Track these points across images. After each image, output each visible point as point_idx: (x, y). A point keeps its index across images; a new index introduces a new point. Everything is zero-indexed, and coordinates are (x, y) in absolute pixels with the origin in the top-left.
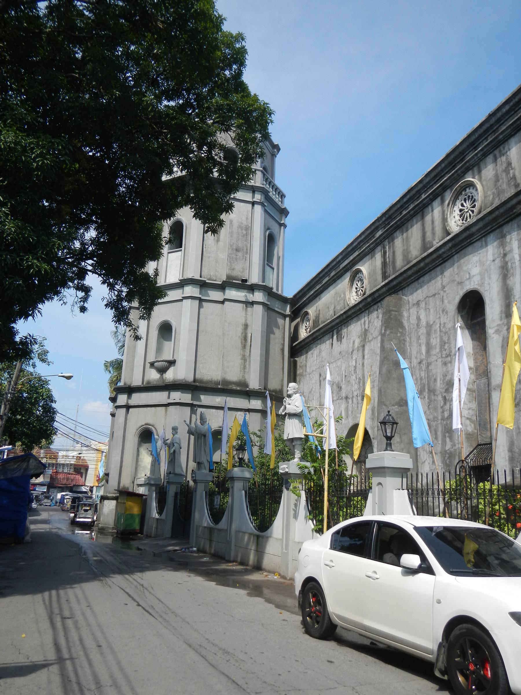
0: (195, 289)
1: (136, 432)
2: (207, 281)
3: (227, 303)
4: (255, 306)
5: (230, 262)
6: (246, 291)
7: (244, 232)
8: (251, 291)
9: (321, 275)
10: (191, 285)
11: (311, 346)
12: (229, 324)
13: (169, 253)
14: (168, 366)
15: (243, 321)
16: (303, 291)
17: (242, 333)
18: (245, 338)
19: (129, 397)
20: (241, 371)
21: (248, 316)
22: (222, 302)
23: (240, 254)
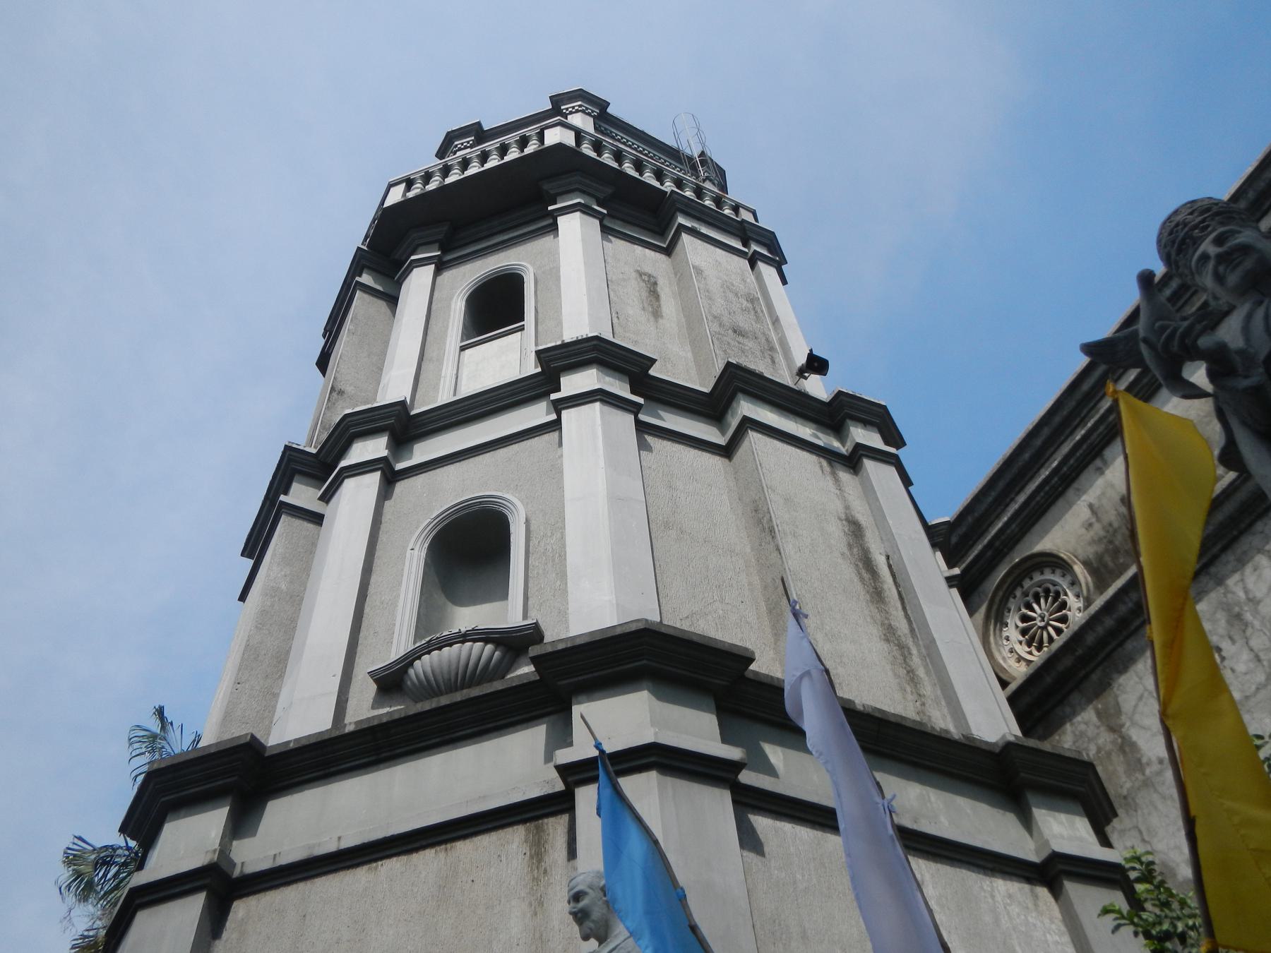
0: (611, 379)
2: (653, 372)
3: (753, 437)
4: (869, 465)
5: (725, 351)
6: (814, 426)
8: (829, 431)
9: (1086, 387)
10: (595, 366)
11: (1129, 645)
13: (463, 349)
14: (500, 661)
15: (838, 506)
16: (970, 519)
17: (850, 546)
19: (241, 823)
21: (851, 498)
22: (727, 451)
23: (749, 344)
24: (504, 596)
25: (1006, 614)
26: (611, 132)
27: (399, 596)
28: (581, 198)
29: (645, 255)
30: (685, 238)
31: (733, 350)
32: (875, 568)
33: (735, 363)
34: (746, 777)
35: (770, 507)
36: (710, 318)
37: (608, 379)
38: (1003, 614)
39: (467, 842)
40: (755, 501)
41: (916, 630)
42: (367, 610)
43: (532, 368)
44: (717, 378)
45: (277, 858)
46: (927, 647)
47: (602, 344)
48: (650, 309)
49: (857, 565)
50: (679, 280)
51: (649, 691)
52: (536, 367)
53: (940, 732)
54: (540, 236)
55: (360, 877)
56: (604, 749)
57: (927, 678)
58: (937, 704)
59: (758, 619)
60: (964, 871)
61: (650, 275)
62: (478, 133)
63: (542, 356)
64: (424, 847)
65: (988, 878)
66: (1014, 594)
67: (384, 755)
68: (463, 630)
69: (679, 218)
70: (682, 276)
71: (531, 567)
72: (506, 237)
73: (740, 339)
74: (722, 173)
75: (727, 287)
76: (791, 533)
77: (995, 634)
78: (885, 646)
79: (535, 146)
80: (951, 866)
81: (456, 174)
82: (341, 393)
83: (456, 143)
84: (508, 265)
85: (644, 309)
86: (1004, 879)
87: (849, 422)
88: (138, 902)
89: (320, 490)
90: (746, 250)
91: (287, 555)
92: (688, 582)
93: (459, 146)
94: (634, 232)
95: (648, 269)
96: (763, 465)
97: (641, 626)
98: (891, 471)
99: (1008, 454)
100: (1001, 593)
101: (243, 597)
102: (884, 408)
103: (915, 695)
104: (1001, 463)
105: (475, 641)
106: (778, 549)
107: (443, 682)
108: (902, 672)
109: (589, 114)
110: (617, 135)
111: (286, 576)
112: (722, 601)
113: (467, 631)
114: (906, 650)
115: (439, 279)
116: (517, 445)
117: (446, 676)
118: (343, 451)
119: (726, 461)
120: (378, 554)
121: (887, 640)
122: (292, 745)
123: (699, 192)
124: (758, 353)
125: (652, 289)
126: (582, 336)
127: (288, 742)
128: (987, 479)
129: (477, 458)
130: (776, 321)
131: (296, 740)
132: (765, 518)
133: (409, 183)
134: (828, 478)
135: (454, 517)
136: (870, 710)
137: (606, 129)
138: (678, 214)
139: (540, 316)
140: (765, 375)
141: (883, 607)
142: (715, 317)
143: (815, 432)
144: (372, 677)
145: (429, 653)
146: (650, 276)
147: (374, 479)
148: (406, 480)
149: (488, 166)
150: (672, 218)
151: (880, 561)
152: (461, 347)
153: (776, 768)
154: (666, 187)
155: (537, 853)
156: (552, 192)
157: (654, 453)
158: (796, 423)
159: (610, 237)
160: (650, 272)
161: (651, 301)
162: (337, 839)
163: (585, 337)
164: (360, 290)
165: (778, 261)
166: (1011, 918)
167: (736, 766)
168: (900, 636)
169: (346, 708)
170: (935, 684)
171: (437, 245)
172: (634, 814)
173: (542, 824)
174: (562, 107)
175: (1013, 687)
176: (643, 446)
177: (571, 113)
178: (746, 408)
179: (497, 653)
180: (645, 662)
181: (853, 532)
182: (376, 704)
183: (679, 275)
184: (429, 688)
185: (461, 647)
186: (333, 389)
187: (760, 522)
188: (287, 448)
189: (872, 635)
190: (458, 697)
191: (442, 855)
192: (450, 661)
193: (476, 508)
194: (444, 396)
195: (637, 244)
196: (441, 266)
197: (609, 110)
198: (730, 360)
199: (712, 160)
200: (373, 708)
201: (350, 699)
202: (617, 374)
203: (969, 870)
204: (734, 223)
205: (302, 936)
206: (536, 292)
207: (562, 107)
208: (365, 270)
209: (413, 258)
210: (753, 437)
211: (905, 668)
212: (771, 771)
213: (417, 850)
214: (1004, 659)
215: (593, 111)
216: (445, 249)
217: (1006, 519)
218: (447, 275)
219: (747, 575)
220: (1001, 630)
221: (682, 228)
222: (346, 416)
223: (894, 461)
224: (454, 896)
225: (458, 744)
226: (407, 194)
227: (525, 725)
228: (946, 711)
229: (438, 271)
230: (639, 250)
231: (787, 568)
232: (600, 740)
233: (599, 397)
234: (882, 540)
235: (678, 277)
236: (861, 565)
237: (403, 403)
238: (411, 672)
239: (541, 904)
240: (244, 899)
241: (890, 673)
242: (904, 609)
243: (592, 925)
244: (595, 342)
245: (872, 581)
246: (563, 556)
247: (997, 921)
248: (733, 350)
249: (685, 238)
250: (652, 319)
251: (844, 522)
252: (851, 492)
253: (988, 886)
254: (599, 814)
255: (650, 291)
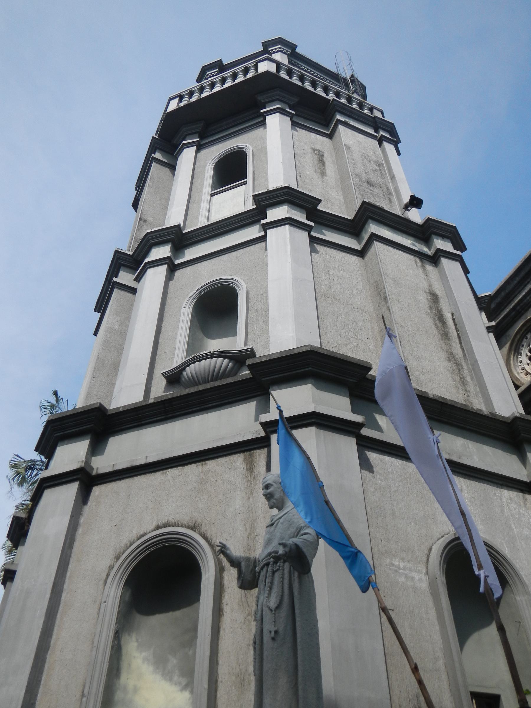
0: (295, 212)
1: (111, 568)
2: (319, 207)
3: (377, 245)
4: (444, 261)
6: (413, 239)
7: (375, 167)
8: (421, 242)
10: (286, 204)
12: (395, 281)
13: (212, 195)
14: (232, 368)
16: (503, 294)
17: (431, 308)
18: (440, 317)
20: (457, 388)
22: (361, 254)
23: (377, 191)
24: (234, 334)
25: (521, 348)
26: (298, 64)
27: (177, 333)
28: (280, 105)
29: (317, 139)
30: (341, 127)
31: (367, 195)
32: (445, 320)
33: (368, 202)
34: (365, 432)
35: (385, 285)
36: (354, 176)
37: (294, 212)
38: (519, 348)
39: (213, 461)
40: (376, 282)
41: (467, 355)
42: (161, 340)
43: (251, 205)
44: (357, 211)
45: (115, 466)
46: (473, 365)
47: (290, 191)
48: (319, 171)
49: (434, 318)
50: (336, 153)
51: (312, 384)
52: (253, 205)
53: (477, 411)
54: (256, 128)
55: (157, 477)
56: (282, 409)
57: (471, 382)
58: (476, 395)
59: (376, 348)
60: (485, 485)
61: (320, 150)
62: (220, 66)
63: (256, 198)
64: (191, 463)
65: (499, 489)
66: (526, 337)
67: (169, 416)
68: (212, 351)
69: (337, 116)
70: (338, 151)
71: (249, 318)
72: (237, 129)
73: (372, 188)
74: (363, 88)
75: (365, 157)
76: (396, 300)
77: (514, 359)
78: (448, 364)
79: (253, 73)
80: (478, 482)
81: (207, 91)
82: (145, 221)
83: (208, 73)
84: (237, 146)
85: (315, 171)
86: (508, 490)
87: (433, 236)
88: (45, 485)
89: (134, 275)
90: (376, 135)
91: (118, 310)
92: (337, 327)
93: (209, 75)
94: (311, 125)
95: (318, 147)
96: (382, 261)
97: (308, 349)
98: (457, 265)
99: (528, 256)
100: (518, 337)
101: (96, 334)
102: (455, 228)
103: (464, 391)
104: (523, 261)
105: (218, 357)
106: (389, 309)
107: (202, 379)
108: (458, 378)
109: (285, 53)
110: (301, 66)
111: (117, 322)
112: (356, 338)
113: (214, 352)
114: (460, 366)
115: (199, 155)
116: (242, 249)
117: (203, 376)
118: (146, 254)
119: (360, 259)
120: (166, 310)
121: (450, 361)
122: (121, 409)
123: (349, 99)
124: (382, 196)
125: (320, 159)
126: (279, 186)
127: (119, 408)
128: (515, 270)
129: (220, 257)
130: (393, 177)
131: (123, 407)
132: (382, 292)
133: (181, 97)
134: (420, 269)
135: (207, 290)
136: (437, 398)
137: (295, 62)
138: (337, 113)
139: (256, 175)
140: (385, 209)
141: (448, 342)
142: (357, 175)
143: (414, 242)
144: (163, 376)
145: (193, 363)
146: (319, 151)
147: (163, 269)
148: (181, 270)
149: (226, 86)
150: (333, 116)
151: (448, 317)
152: (211, 194)
153: (382, 428)
154: (330, 97)
155: (250, 468)
156: (263, 101)
157: (320, 254)
158: (402, 237)
159: (296, 128)
160: (319, 149)
161: (320, 166)
162: (145, 458)
163: (280, 187)
164: (155, 162)
165: (395, 141)
166: (510, 510)
167: (360, 425)
168: (457, 358)
169: (150, 392)
170: (476, 385)
171: (197, 135)
172: (297, 443)
173: (253, 453)
174: (269, 49)
175: (522, 389)
176: (313, 250)
177: (274, 53)
178: (373, 228)
179: (230, 364)
180: (310, 368)
181: (433, 300)
182: (166, 390)
183: (336, 150)
184: (194, 381)
185: (211, 360)
186: (140, 219)
187: (379, 294)
188: (116, 252)
189: (441, 358)
190: (209, 386)
191: (200, 467)
192: (205, 368)
193: (220, 285)
194: (202, 223)
195: (312, 132)
196: (200, 147)
197: (297, 50)
198: (365, 200)
199: (358, 80)
200: (164, 392)
201: (152, 387)
202: (299, 209)
203: (489, 484)
204: (371, 119)
205: (128, 505)
206: (253, 162)
207: (269, 49)
208: (157, 150)
209: (184, 142)
210: (377, 245)
211: (459, 376)
212: (379, 429)
213: (187, 464)
214: (518, 373)
215: (287, 51)
216: (202, 137)
217: (524, 293)
218: (204, 153)
219: (371, 323)
220: (517, 357)
221: (339, 122)
222: (148, 234)
223: (459, 259)
224: (206, 488)
225: (208, 411)
226: (180, 104)
227: (245, 401)
228: (481, 400)
229: (198, 150)
230: (313, 135)
231: (394, 320)
232: (280, 405)
233: (288, 222)
234: (450, 304)
235: (336, 151)
236: (437, 319)
237: (178, 226)
238: (184, 373)
239: (252, 493)
240: (99, 486)
241: (450, 378)
242: (461, 343)
243: (274, 501)
244: (286, 190)
245: (442, 328)
246: (267, 312)
247: (502, 512)
248: (367, 195)
249: (341, 127)
250: (320, 177)
251: (428, 294)
252: (433, 277)
253: (499, 493)
254: (278, 443)
255: (320, 160)
